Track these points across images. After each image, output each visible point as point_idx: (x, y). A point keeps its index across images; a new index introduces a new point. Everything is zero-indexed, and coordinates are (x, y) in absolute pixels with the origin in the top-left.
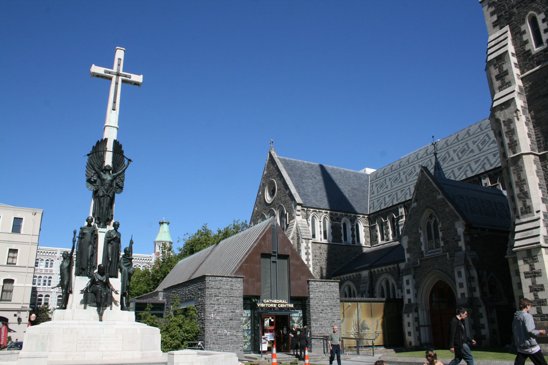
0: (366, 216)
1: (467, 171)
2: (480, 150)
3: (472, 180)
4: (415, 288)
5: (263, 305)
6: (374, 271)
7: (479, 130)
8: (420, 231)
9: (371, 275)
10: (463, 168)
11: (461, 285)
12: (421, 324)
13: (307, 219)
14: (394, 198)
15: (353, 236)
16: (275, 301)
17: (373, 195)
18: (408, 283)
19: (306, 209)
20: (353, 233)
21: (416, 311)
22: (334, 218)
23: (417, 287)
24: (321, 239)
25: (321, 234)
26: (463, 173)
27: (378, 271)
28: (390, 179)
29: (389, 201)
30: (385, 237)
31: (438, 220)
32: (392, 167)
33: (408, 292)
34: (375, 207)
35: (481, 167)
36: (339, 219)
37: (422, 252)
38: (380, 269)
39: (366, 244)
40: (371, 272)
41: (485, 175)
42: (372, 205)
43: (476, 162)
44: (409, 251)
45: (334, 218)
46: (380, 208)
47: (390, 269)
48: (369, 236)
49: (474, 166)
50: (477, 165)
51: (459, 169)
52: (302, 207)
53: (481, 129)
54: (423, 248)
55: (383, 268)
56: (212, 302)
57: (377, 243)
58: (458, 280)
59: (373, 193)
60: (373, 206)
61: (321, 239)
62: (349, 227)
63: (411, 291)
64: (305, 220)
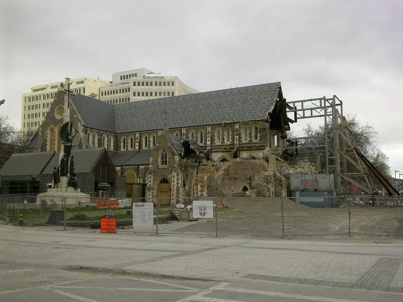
0: (115, 134)
1: (175, 123)
2: (183, 113)
3: (177, 129)
4: (154, 180)
5: (100, 185)
6: (124, 168)
7: (183, 101)
8: (158, 157)
9: (122, 169)
10: (174, 121)
11: (174, 181)
12: (154, 195)
13: (86, 134)
14: (133, 127)
15: (108, 145)
16: (104, 184)
17: (118, 121)
18: (150, 178)
19: (86, 128)
20: (108, 143)
21: (153, 190)
22: (100, 134)
23: (154, 180)
24: (92, 146)
25: (92, 143)
26: (173, 124)
27: (126, 167)
28: (130, 113)
29: (130, 128)
30: (126, 148)
31: (167, 154)
32: (130, 105)
33: (150, 182)
34: (121, 129)
35: (182, 123)
36: (101, 135)
37: (158, 166)
38: (128, 167)
39: (113, 150)
40: (122, 168)
41: (184, 128)
42: (118, 128)
43: (181, 120)
44: (152, 164)
45: (100, 134)
46: (125, 131)
47: (133, 167)
48: (116, 145)
49: (179, 122)
50: (181, 122)
51: (172, 121)
52: (85, 127)
53: (184, 100)
54: (159, 164)
55: (130, 167)
56: (85, 184)
57: (120, 150)
58: (173, 179)
59: (118, 119)
60: (120, 129)
61: (92, 146)
62: (106, 140)
63: (151, 181)
64: (85, 135)
